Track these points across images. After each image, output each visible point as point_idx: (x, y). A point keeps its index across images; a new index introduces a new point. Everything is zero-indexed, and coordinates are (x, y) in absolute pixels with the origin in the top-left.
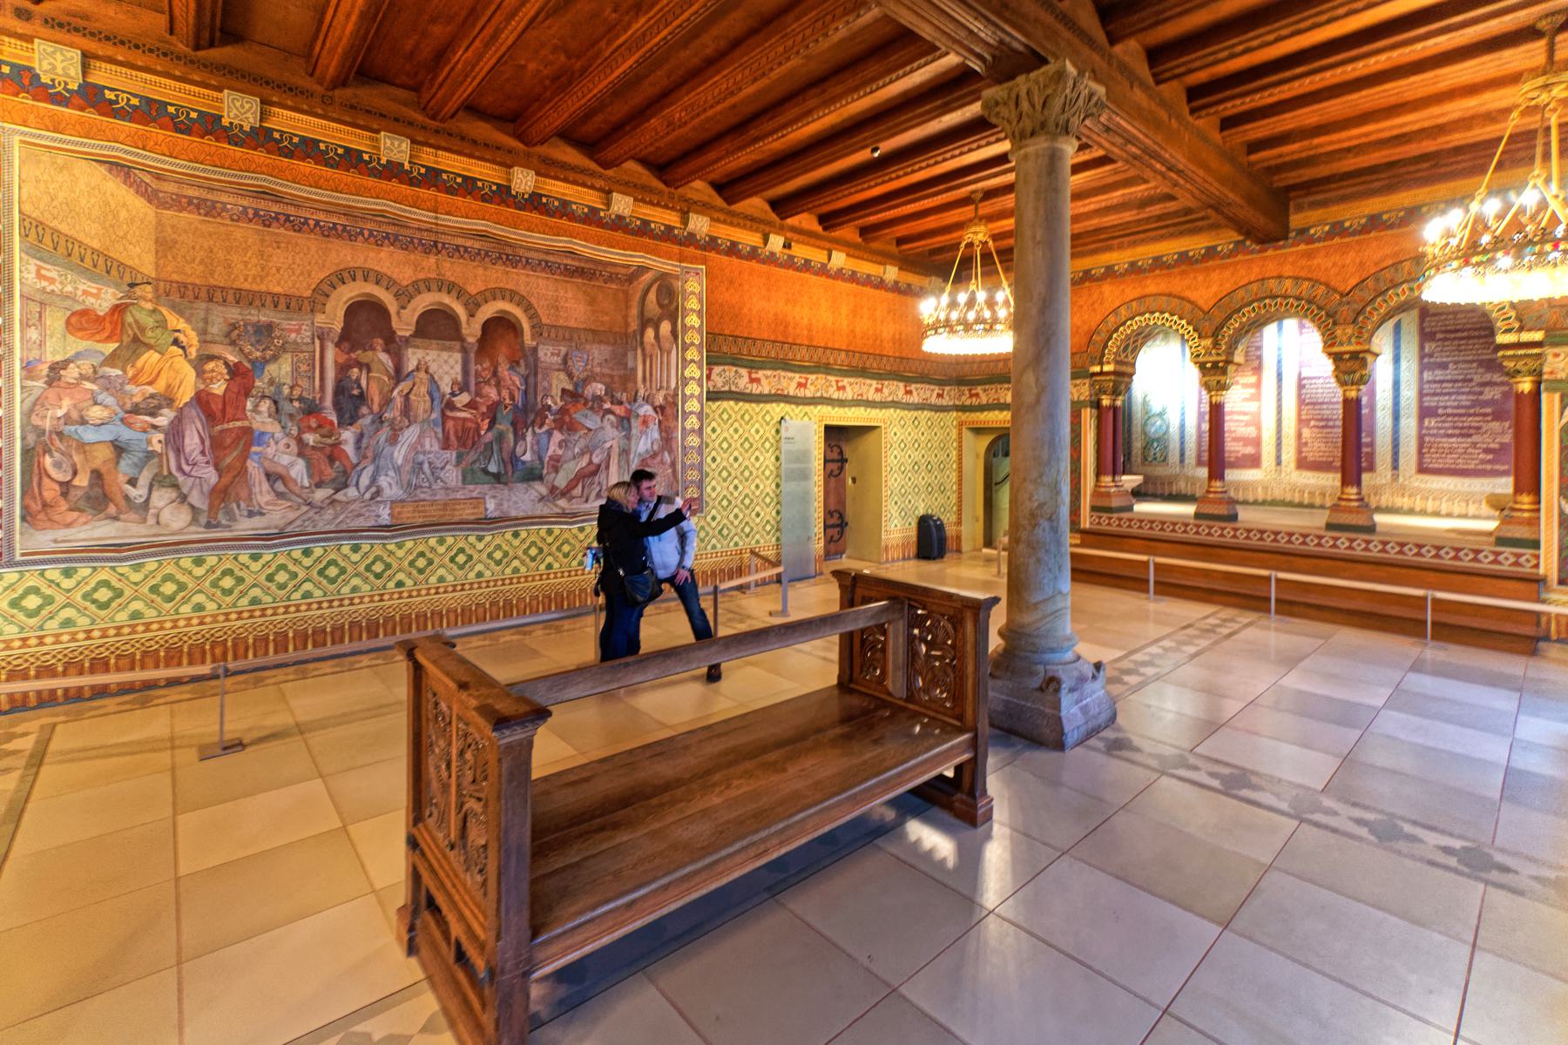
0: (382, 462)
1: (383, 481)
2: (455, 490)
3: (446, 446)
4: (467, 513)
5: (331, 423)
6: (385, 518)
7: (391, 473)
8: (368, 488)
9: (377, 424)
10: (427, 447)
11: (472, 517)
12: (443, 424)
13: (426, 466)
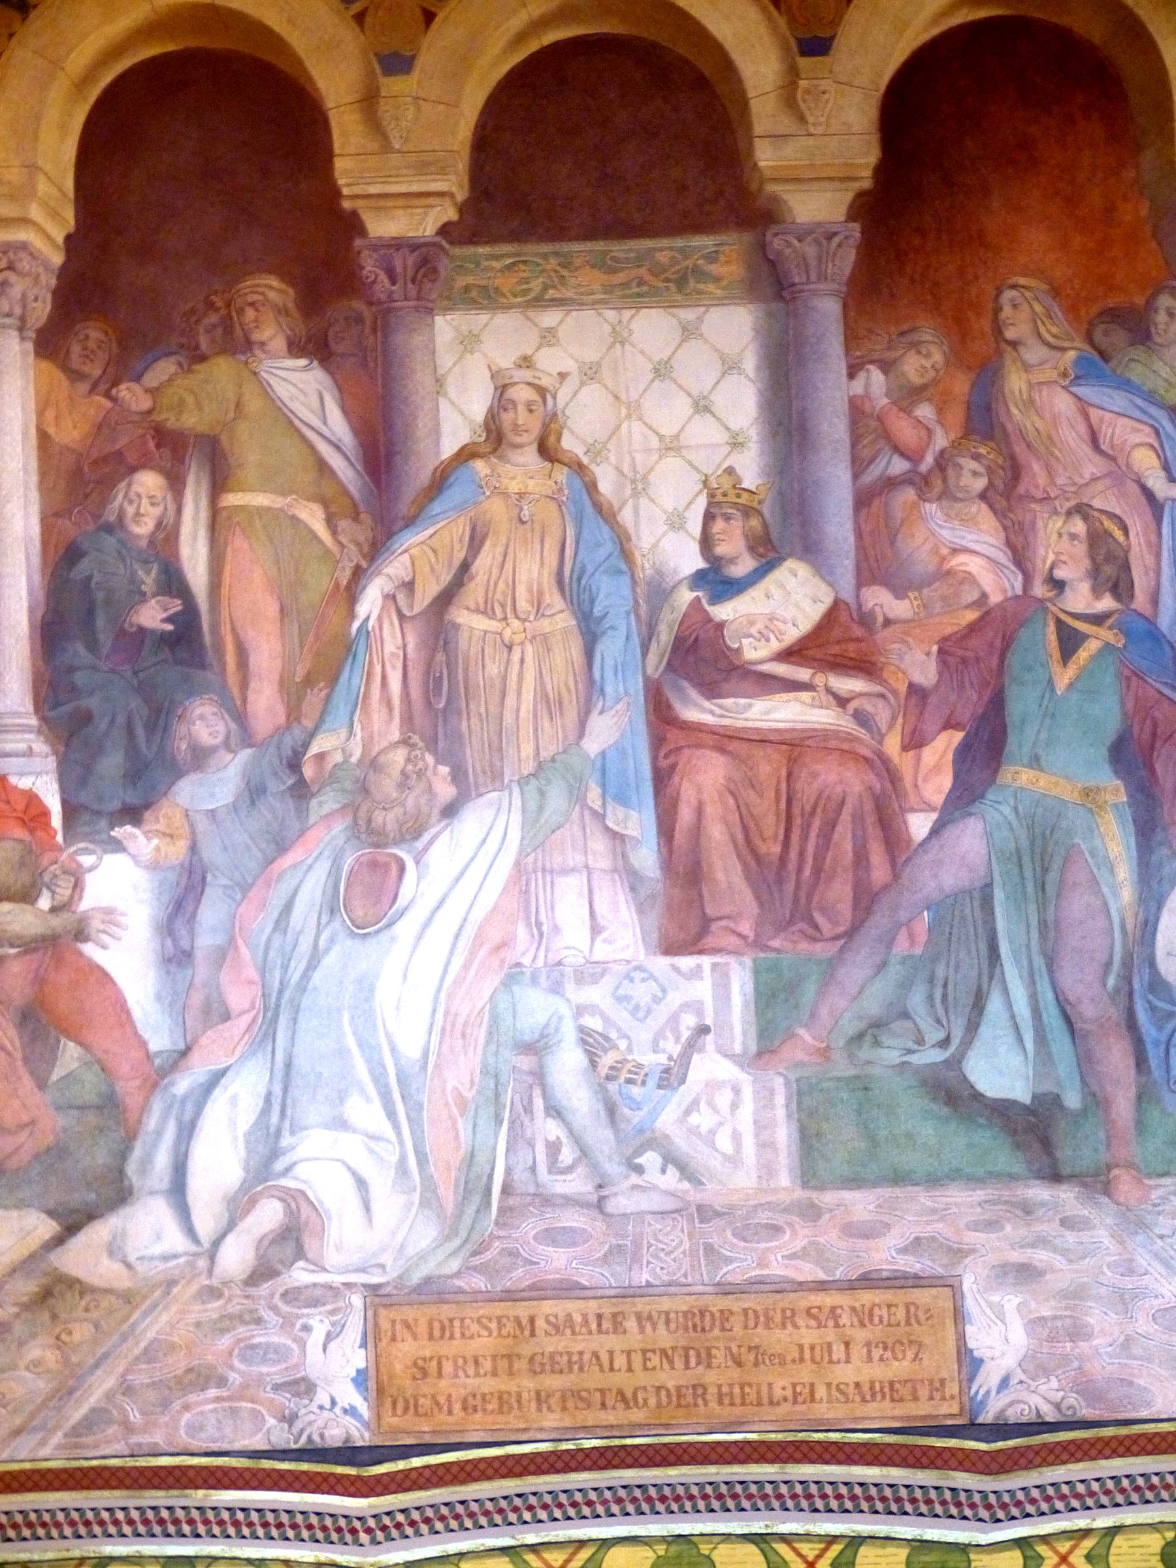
0: (310, 1041)
1: (320, 1165)
2: (755, 1225)
3: (686, 928)
4: (851, 1384)
5: (32, 813)
6: (340, 1408)
7: (365, 1112)
8: (239, 1205)
9: (276, 805)
10: (573, 935)
11: (882, 1412)
12: (662, 779)
13: (567, 1066)
